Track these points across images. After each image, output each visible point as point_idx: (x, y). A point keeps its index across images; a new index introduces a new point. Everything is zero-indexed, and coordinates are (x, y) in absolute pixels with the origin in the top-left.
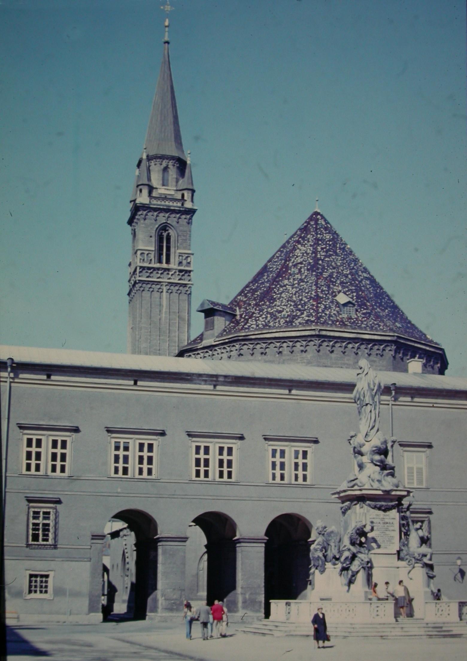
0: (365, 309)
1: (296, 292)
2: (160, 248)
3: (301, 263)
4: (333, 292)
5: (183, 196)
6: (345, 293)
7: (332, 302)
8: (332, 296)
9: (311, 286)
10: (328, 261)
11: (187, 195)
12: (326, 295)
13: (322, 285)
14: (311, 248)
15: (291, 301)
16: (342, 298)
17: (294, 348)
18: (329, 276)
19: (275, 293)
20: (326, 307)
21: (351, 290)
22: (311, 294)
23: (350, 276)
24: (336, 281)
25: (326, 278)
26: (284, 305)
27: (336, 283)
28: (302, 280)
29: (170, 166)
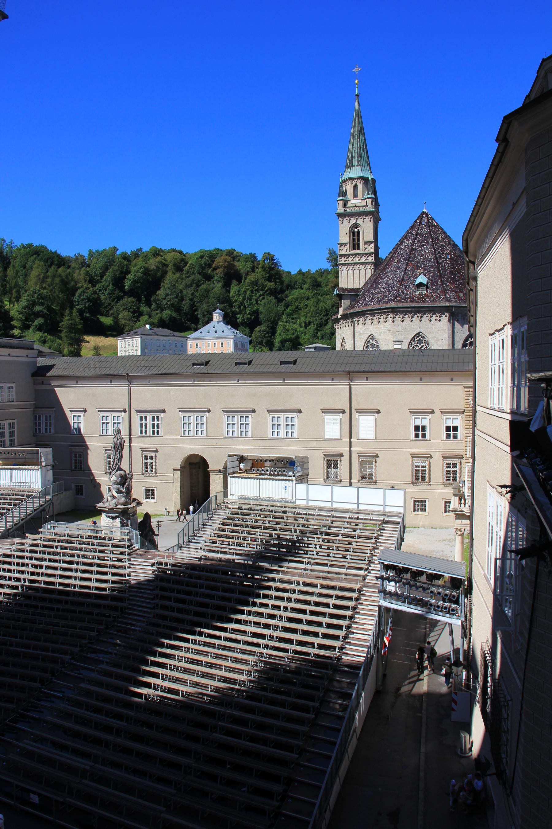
0: (435, 285)
3: (402, 254)
4: (416, 274)
5: (367, 202)
7: (412, 283)
8: (414, 278)
9: (402, 272)
10: (420, 250)
11: (369, 201)
12: (409, 278)
13: (409, 271)
15: (387, 284)
16: (422, 279)
18: (417, 262)
19: (381, 278)
20: (406, 287)
23: (432, 260)
24: (421, 265)
25: (414, 264)
26: (383, 288)
27: (420, 267)
28: (398, 268)
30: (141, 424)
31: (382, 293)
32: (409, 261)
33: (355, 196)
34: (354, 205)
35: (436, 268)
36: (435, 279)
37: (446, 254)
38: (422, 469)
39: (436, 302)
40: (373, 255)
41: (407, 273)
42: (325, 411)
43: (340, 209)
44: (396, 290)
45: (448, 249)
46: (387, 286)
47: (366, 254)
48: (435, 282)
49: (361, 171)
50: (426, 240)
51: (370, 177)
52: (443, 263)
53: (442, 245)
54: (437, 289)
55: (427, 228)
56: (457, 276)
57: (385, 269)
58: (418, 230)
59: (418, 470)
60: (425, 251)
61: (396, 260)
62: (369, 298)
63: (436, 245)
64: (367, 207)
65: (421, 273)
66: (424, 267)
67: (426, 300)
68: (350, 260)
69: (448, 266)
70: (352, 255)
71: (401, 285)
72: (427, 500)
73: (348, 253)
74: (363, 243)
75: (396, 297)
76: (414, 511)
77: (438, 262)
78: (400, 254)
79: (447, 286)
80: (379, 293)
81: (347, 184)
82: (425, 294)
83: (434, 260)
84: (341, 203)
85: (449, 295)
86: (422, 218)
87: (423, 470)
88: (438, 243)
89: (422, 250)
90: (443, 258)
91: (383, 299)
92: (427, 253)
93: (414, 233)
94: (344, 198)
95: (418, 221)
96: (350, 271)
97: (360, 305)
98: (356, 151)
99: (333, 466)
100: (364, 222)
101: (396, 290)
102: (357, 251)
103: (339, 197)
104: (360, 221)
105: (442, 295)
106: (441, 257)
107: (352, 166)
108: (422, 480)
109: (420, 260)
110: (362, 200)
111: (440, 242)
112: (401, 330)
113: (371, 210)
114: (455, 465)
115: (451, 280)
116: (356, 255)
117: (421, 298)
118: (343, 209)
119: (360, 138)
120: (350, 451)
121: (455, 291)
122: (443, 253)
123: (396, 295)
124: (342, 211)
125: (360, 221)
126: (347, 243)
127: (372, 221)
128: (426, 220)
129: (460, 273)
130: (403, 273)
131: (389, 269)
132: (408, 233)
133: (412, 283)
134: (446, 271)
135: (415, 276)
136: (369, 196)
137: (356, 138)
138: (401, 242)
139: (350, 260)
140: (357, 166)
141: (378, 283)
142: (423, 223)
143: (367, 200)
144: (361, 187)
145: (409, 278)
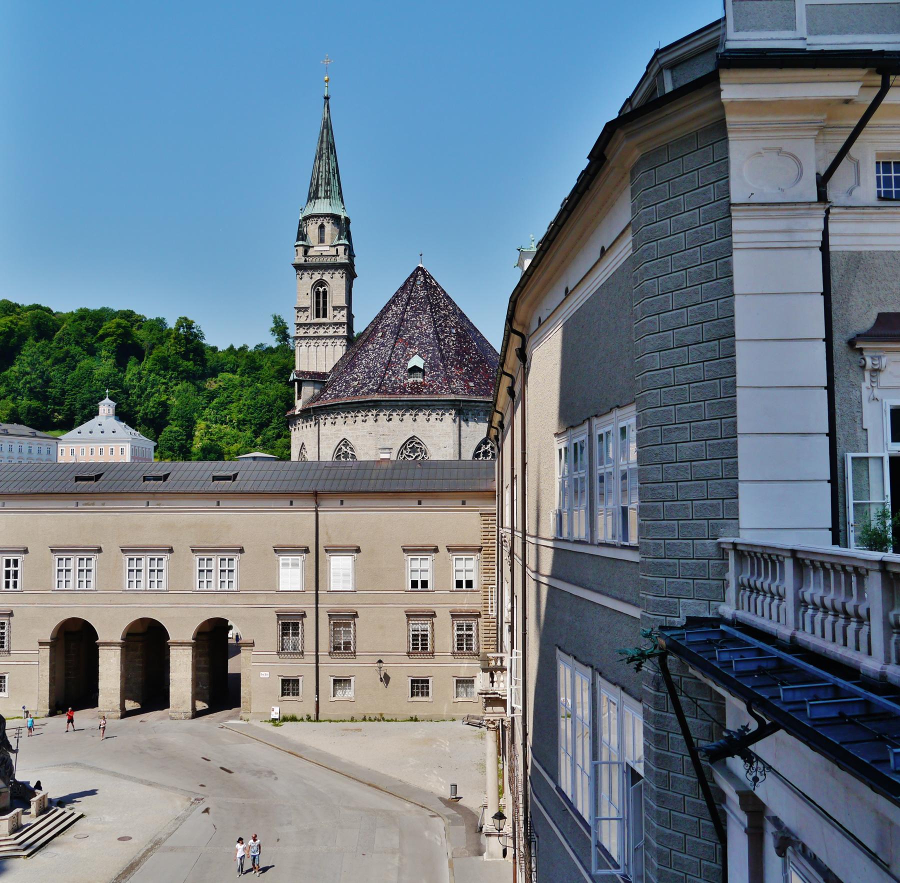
0: (435, 371)
1: (375, 357)
2: (318, 303)
3: (388, 325)
4: (409, 355)
5: (337, 250)
6: (420, 355)
7: (403, 367)
8: (405, 360)
9: (388, 351)
10: (413, 321)
11: (341, 249)
12: (399, 360)
13: (398, 349)
14: (401, 308)
15: (367, 368)
16: (417, 361)
17: (357, 418)
18: (410, 337)
19: (358, 358)
20: (394, 373)
21: (428, 351)
22: (386, 359)
23: (431, 336)
25: (405, 340)
27: (414, 345)
28: (383, 345)
29: (325, 224)
30: (8, 573)
31: (359, 380)
32: (398, 335)
33: (322, 241)
34: (319, 254)
35: (436, 346)
36: (435, 362)
37: (450, 328)
38: (422, 633)
39: (437, 394)
40: (345, 326)
41: (395, 352)
42: (279, 550)
43: (300, 260)
44: (380, 376)
45: (452, 321)
46: (367, 370)
47: (336, 324)
48: (435, 366)
49: (330, 205)
50: (422, 307)
51: (343, 215)
52: (447, 340)
53: (444, 314)
54: (438, 376)
55: (423, 290)
56: (466, 359)
57: (365, 346)
58: (411, 292)
59: (418, 635)
60: (421, 323)
61: (380, 334)
62: (341, 387)
63: (436, 315)
64: (338, 258)
65: (416, 353)
66: (419, 344)
67: (422, 391)
68: (311, 332)
69: (453, 344)
70: (315, 324)
71: (386, 370)
72: (431, 680)
73: (307, 322)
74: (332, 309)
75: (380, 387)
76: (412, 695)
77: (439, 340)
78: (386, 326)
79: (452, 372)
80: (355, 380)
81: (310, 223)
82: (421, 383)
83: (434, 335)
84: (301, 250)
85: (454, 384)
86: (417, 276)
87: (423, 635)
88: (439, 312)
89: (417, 321)
90: (446, 333)
91: (362, 388)
92: (424, 325)
93: (405, 296)
94: (304, 243)
95: (412, 280)
96: (312, 347)
97: (328, 396)
98: (324, 177)
99: (291, 632)
100: (332, 278)
101: (380, 376)
102: (322, 320)
103: (298, 240)
104: (327, 277)
105: (446, 385)
106: (443, 332)
107: (318, 198)
108: (422, 649)
109: (413, 334)
110: (331, 246)
111: (442, 310)
112: (387, 433)
113: (344, 261)
114: (469, 628)
115: (457, 364)
116: (320, 325)
117: (416, 389)
118: (303, 259)
119: (329, 159)
120: (317, 608)
121: (462, 379)
122: (446, 326)
123: (381, 383)
124: (302, 261)
125: (327, 277)
126: (308, 308)
127: (344, 278)
128: (422, 279)
129: (469, 354)
130: (389, 353)
131: (370, 346)
132: (396, 296)
133: (403, 367)
134: (450, 352)
135: (406, 357)
136: (341, 242)
137: (324, 158)
138: (387, 309)
139: (311, 332)
140: (324, 198)
141: (355, 366)
142: (418, 283)
143: (338, 247)
144: (330, 229)
145: (399, 360)
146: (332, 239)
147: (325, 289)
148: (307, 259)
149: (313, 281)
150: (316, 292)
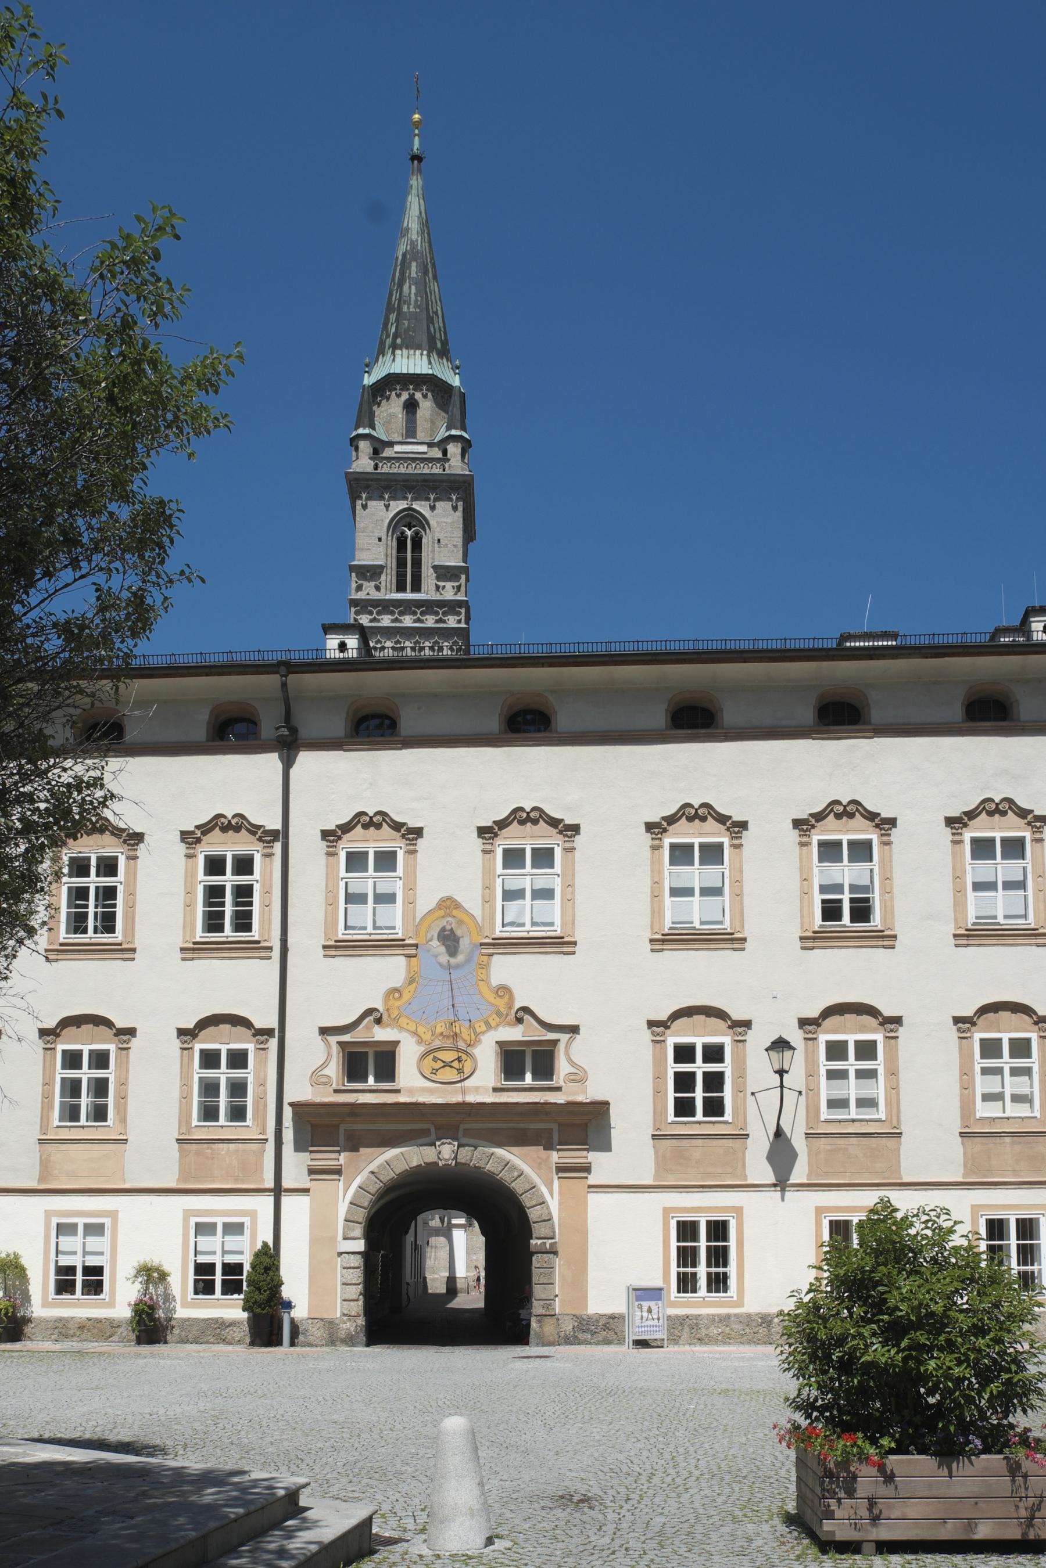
2: (401, 563)
5: (445, 452)
11: (454, 449)
29: (418, 396)
33: (411, 430)
43: (363, 463)
47: (441, 604)
84: (364, 446)
104: (421, 507)
110: (430, 445)
116: (407, 607)
125: (421, 507)
136: (454, 432)
146: (433, 430)
147: (417, 533)
148: (380, 465)
149: (391, 515)
150: (398, 539)
